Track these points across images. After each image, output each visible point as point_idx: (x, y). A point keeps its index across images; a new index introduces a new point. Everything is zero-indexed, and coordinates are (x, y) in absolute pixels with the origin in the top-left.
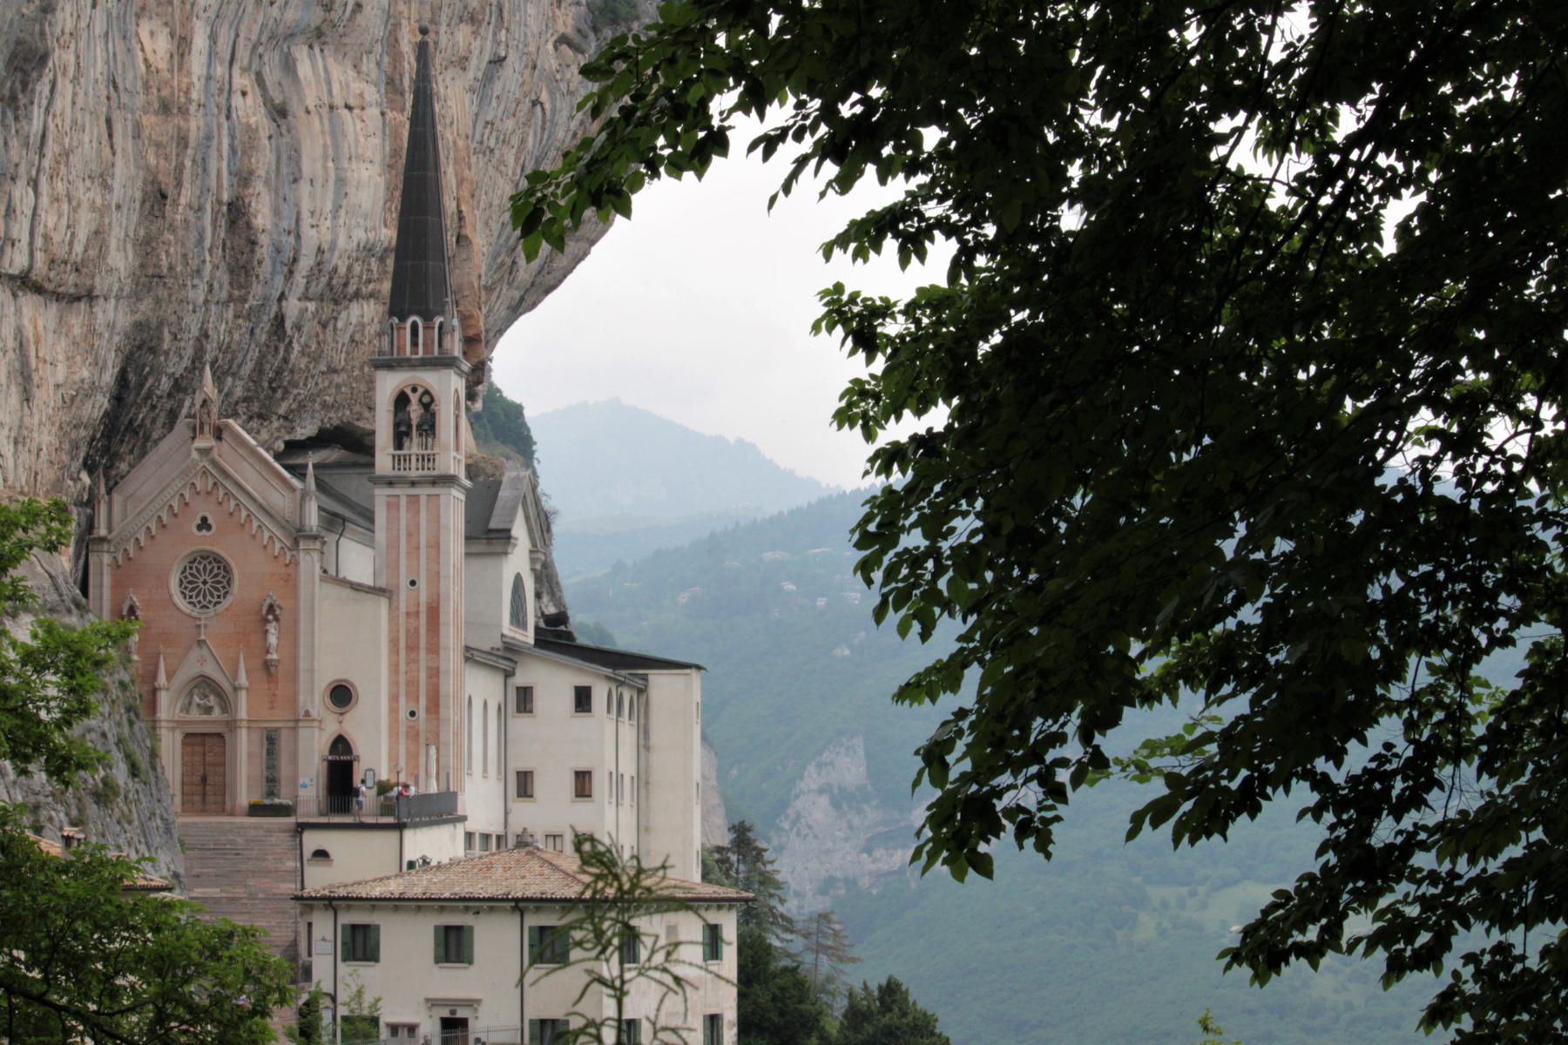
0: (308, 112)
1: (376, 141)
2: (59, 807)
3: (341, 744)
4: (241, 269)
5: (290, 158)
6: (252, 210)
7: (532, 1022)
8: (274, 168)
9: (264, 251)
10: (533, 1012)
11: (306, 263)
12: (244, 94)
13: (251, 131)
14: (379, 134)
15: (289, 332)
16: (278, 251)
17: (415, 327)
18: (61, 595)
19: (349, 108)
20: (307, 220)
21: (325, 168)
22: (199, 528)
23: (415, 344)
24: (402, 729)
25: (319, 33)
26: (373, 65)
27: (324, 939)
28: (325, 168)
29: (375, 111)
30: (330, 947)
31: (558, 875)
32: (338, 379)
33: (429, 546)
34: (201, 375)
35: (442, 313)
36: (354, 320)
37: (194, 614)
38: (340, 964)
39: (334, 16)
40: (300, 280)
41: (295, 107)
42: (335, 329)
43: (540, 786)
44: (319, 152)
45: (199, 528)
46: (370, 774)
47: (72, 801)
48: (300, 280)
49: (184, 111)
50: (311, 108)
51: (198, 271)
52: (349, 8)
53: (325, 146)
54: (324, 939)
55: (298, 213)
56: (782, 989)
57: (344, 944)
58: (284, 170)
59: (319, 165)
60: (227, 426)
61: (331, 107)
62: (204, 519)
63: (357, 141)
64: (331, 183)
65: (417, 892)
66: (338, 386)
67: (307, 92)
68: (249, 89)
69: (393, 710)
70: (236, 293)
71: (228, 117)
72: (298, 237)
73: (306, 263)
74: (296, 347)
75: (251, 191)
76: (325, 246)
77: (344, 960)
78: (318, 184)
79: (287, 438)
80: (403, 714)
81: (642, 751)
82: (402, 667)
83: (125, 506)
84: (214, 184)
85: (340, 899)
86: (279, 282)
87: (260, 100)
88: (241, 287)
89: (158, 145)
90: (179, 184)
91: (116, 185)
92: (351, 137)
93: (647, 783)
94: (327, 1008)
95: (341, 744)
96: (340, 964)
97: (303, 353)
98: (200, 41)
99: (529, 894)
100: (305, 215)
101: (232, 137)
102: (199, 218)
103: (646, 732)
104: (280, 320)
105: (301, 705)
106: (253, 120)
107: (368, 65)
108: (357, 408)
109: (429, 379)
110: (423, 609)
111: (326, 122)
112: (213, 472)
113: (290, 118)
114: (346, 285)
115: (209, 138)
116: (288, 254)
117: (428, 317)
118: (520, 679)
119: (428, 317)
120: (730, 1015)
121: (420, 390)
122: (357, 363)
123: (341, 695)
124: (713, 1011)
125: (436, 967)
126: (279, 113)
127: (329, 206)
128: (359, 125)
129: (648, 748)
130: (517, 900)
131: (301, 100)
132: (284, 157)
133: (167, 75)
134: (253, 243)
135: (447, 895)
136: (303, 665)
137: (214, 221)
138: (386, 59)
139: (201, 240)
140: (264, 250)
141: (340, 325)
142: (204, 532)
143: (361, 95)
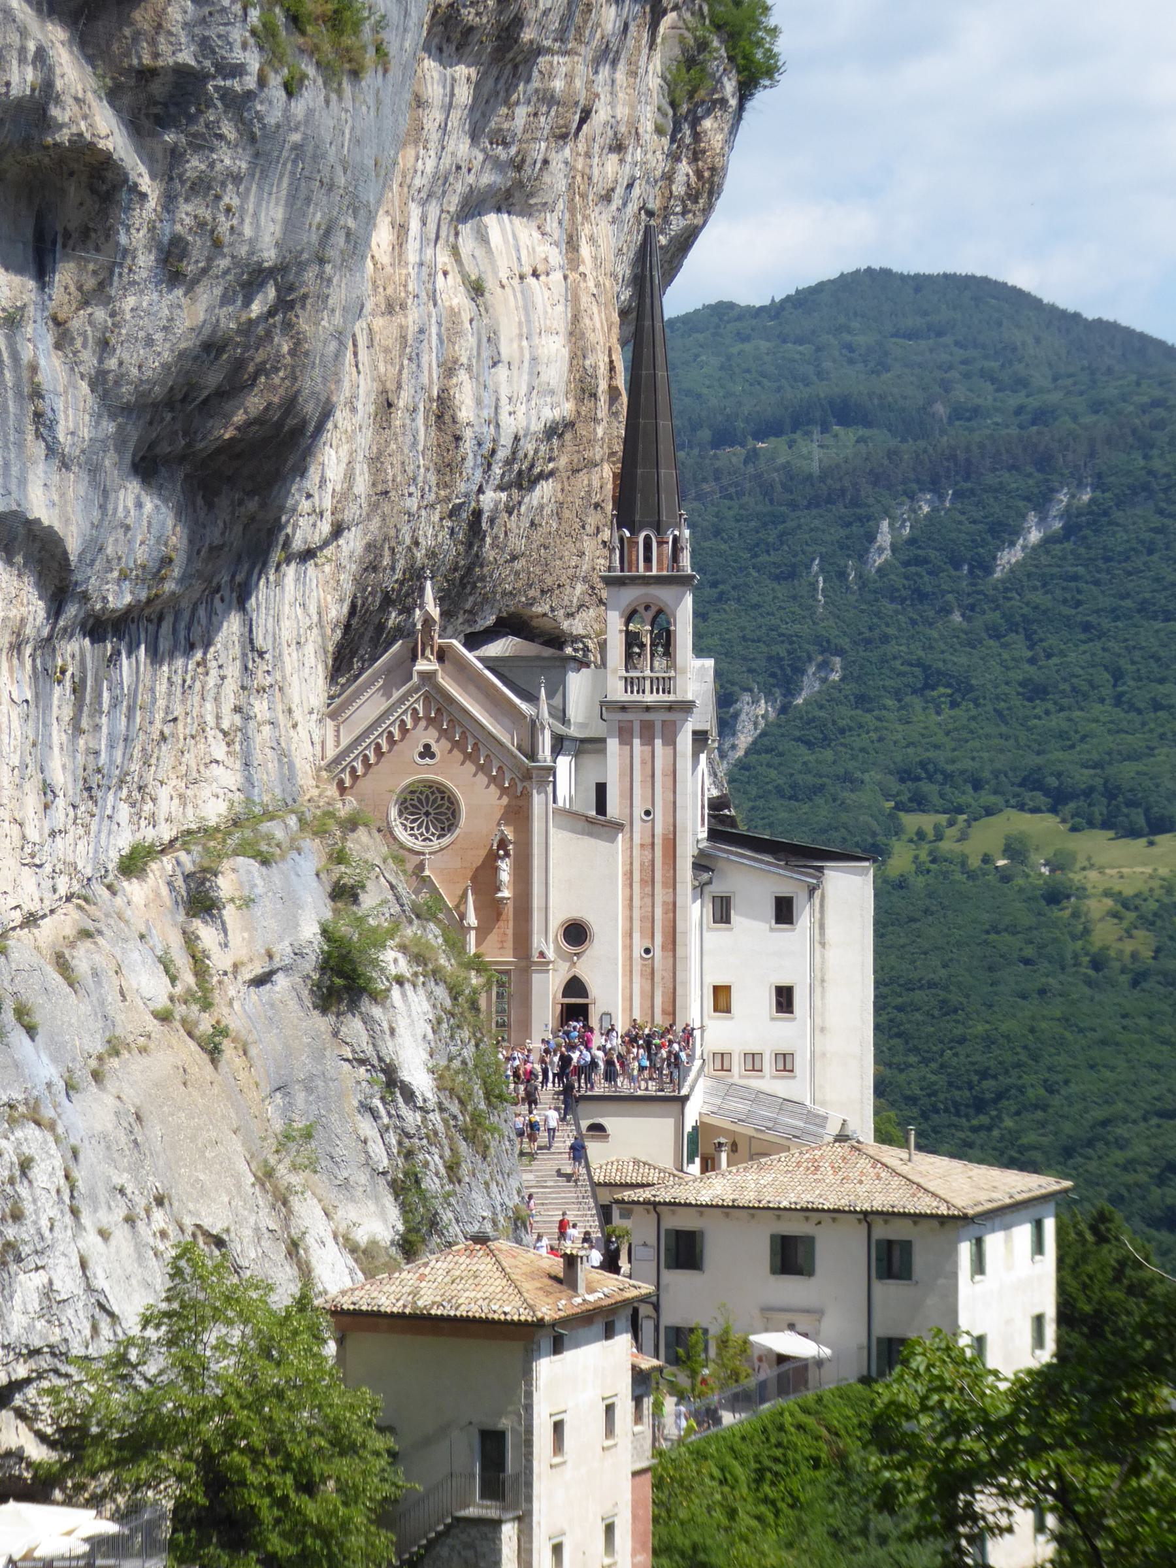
0: (503, 287)
1: (560, 308)
2: (433, 1149)
3: (575, 987)
4: (448, 468)
5: (489, 339)
6: (457, 403)
7: (879, 1340)
8: (475, 353)
9: (468, 445)
10: (879, 1331)
11: (502, 454)
12: (445, 274)
13: (454, 314)
14: (562, 300)
15: (484, 526)
16: (479, 444)
17: (647, 540)
18: (402, 905)
19: (535, 274)
20: (505, 408)
21: (521, 348)
22: (422, 756)
23: (648, 559)
24: (637, 968)
25: (508, 193)
26: (555, 224)
27: (645, 1245)
28: (521, 348)
29: (557, 276)
30: (652, 1253)
31: (896, 1181)
32: (517, 565)
33: (664, 775)
34: (421, 596)
35: (678, 526)
36: (535, 503)
37: (417, 848)
38: (664, 1271)
39: (525, 176)
40: (497, 470)
41: (490, 284)
42: (519, 514)
43: (737, 1000)
44: (516, 331)
45: (422, 756)
46: (606, 1019)
47: (445, 1142)
48: (497, 470)
49: (403, 306)
50: (505, 281)
51: (414, 479)
52: (538, 166)
53: (520, 323)
54: (645, 1245)
55: (498, 399)
56: (1090, 1277)
57: (667, 1249)
58: (485, 354)
59: (515, 345)
60: (450, 646)
61: (522, 277)
62: (427, 747)
63: (546, 312)
64: (526, 364)
65: (748, 1197)
66: (517, 573)
67: (499, 263)
68: (449, 268)
69: (629, 947)
70: (442, 493)
71: (435, 305)
72: (498, 426)
73: (502, 454)
74: (488, 540)
75: (454, 380)
76: (521, 433)
77: (668, 1267)
78: (514, 367)
79: (469, 630)
80: (638, 951)
81: (817, 946)
82: (637, 902)
83: (338, 731)
84: (426, 381)
85: (665, 1204)
86: (478, 474)
87: (459, 279)
88: (446, 486)
89: (387, 350)
90: (399, 387)
91: (360, 407)
92: (540, 307)
93: (823, 981)
94: (648, 1317)
95: (575, 987)
96: (664, 1271)
97: (493, 546)
98: (414, 226)
99: (877, 1205)
100: (504, 401)
101: (439, 324)
102: (413, 420)
103: (822, 927)
104: (477, 514)
105: (535, 945)
106: (455, 302)
107: (552, 225)
108: (531, 593)
109: (663, 594)
110: (658, 841)
111: (519, 295)
112: (438, 697)
113: (487, 295)
114: (532, 466)
115: (421, 331)
116: (489, 445)
117: (659, 528)
118: (717, 888)
119: (659, 528)
120: (1051, 1313)
121: (654, 610)
122: (534, 546)
123: (576, 933)
124: (1037, 1311)
125: (773, 1278)
126: (477, 289)
127: (524, 389)
128: (547, 294)
129: (823, 945)
130: (865, 1214)
131: (495, 273)
132: (485, 340)
133: (389, 269)
134: (458, 438)
135: (785, 1204)
136: (537, 902)
137: (426, 418)
138: (567, 216)
139: (415, 443)
140: (467, 445)
141: (523, 509)
142: (428, 760)
143: (546, 260)
